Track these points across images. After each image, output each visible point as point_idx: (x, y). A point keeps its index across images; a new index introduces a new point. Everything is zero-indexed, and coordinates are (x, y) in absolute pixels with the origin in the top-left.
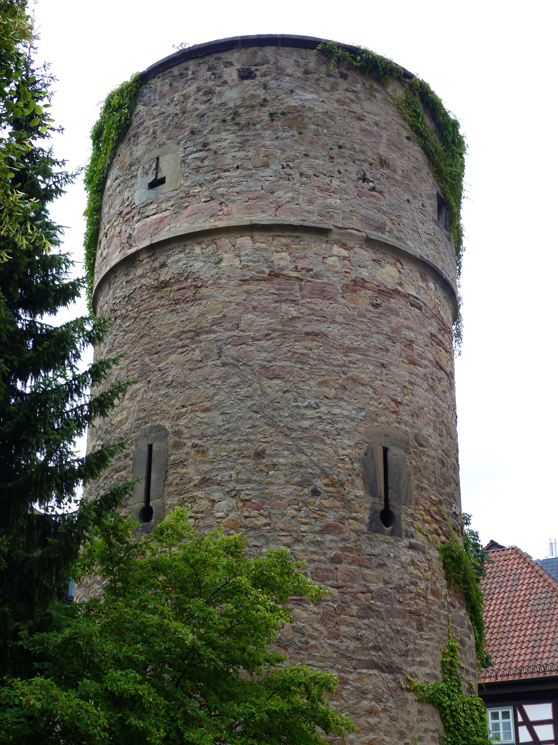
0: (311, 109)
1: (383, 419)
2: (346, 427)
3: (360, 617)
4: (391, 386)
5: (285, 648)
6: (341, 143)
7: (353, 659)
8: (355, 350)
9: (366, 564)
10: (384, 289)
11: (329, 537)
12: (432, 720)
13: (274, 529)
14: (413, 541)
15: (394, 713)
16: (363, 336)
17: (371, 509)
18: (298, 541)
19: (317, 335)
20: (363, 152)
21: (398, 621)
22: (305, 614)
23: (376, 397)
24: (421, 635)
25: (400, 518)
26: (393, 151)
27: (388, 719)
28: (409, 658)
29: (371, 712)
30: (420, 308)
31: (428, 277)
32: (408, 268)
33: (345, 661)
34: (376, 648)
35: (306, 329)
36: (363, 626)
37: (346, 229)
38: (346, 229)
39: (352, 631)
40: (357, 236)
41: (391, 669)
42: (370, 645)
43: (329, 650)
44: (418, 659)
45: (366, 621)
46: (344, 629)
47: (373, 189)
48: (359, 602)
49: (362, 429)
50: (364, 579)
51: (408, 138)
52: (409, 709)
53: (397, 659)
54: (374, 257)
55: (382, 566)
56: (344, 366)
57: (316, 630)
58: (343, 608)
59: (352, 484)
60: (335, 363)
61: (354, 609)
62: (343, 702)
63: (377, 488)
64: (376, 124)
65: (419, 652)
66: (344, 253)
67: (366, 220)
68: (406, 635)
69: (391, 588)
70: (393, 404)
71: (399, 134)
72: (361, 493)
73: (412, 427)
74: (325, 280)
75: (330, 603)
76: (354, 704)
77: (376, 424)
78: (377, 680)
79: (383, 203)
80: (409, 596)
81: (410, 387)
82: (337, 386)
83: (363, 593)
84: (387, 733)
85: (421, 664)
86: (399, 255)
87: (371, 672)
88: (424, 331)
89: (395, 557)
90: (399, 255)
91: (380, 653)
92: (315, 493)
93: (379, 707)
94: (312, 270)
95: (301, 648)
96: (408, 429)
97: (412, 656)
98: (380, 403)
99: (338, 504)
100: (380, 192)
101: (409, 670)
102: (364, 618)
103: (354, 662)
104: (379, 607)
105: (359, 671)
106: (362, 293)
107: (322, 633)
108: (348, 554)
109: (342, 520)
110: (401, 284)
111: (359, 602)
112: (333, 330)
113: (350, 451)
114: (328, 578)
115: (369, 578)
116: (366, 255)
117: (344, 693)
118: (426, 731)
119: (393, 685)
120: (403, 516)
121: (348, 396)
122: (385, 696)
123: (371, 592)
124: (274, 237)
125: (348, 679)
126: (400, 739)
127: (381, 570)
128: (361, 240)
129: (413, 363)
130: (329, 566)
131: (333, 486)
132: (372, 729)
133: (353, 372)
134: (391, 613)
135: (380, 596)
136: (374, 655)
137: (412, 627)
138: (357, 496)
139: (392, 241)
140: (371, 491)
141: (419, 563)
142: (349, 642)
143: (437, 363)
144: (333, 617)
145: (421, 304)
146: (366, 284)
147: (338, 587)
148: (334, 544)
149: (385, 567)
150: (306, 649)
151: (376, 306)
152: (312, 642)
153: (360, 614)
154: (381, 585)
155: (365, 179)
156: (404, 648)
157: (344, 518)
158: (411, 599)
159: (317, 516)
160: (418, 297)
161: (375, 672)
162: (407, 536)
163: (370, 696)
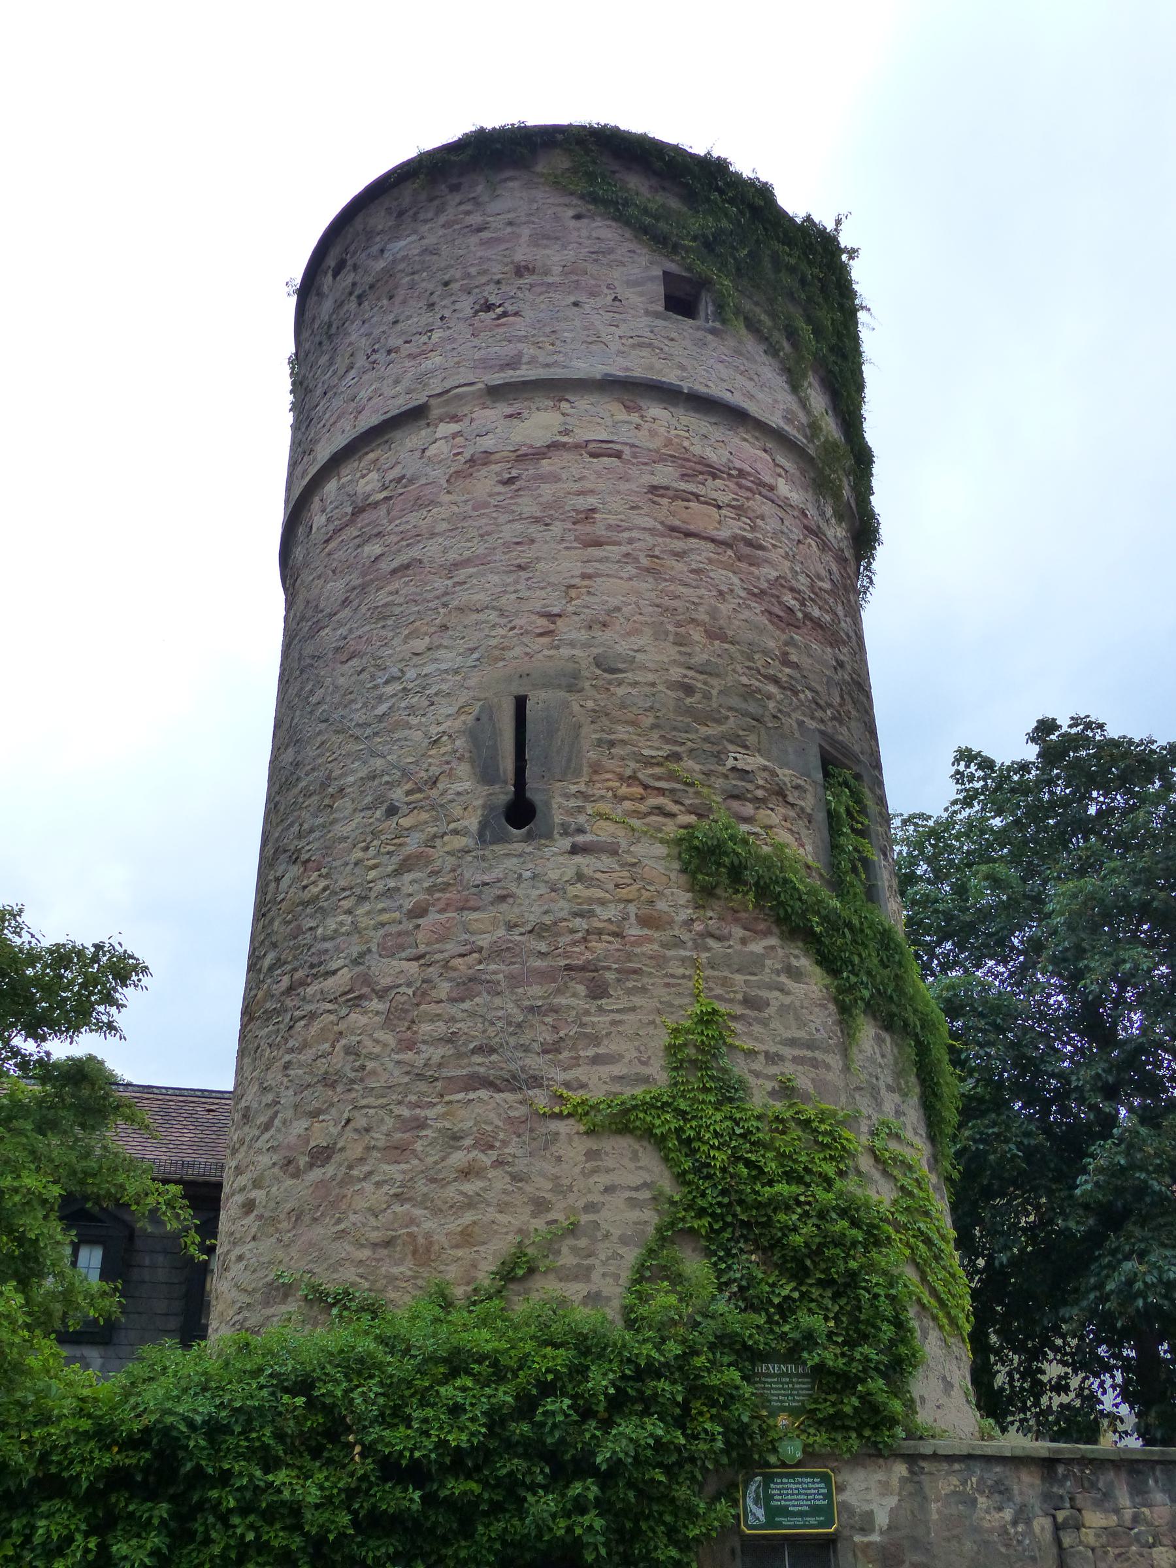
0: (404, 258)
1: (518, 651)
2: (444, 687)
3: (453, 1000)
4: (538, 593)
5: (333, 1086)
6: (447, 277)
7: (437, 1079)
8: (466, 563)
9: (471, 904)
10: (531, 451)
11: (408, 877)
12: (631, 1166)
13: (334, 893)
14: (580, 839)
15: (521, 1166)
16: (481, 536)
17: (484, 806)
18: (363, 899)
19: (407, 567)
20: (485, 272)
21: (536, 990)
22: (364, 1020)
23: (503, 621)
24: (600, 1009)
25: (547, 804)
26: (546, 247)
27: (508, 1179)
28: (565, 1054)
29: (466, 1173)
30: (618, 455)
31: (643, 403)
32: (583, 403)
33: (423, 1086)
34: (485, 1049)
35: (395, 564)
36: (460, 1015)
37: (448, 391)
38: (448, 391)
39: (441, 1028)
40: (473, 393)
41: (511, 1083)
42: (471, 1046)
43: (396, 1073)
44: (591, 1052)
45: (466, 1005)
46: (425, 1028)
47: (505, 314)
48: (454, 974)
49: (471, 682)
50: (467, 931)
51: (578, 217)
52: (561, 1152)
53: (535, 1062)
54: (509, 410)
55: (503, 898)
56: (446, 594)
57: (377, 1041)
58: (422, 995)
59: (450, 776)
60: (430, 596)
61: (444, 988)
62: (416, 1162)
63: (498, 770)
64: (510, 224)
65: (595, 1040)
66: (454, 427)
67: (485, 364)
68: (556, 1012)
69: (522, 934)
70: (543, 622)
71: (556, 218)
72: (467, 785)
73: (586, 646)
74: (423, 481)
75: (403, 989)
76: (436, 1163)
77: (501, 664)
78: (487, 1109)
79: (520, 326)
80: (567, 939)
81: (586, 582)
82: (433, 629)
83: (462, 955)
84: (502, 1208)
85: (596, 1060)
86: (557, 388)
87: (472, 1095)
88: (623, 486)
89: (534, 877)
90: (557, 388)
91: (494, 1057)
92: (392, 811)
93: (486, 1159)
94: (403, 477)
95: (353, 1081)
96: (577, 652)
97: (574, 1048)
98: (512, 629)
99: (425, 816)
100: (516, 314)
101: (561, 1076)
102: (463, 1000)
103: (439, 1084)
104: (495, 973)
105: (447, 1098)
106: (484, 472)
107: (385, 1045)
108: (437, 895)
109: (430, 842)
110: (566, 432)
111: (454, 974)
112: (432, 549)
113: (449, 723)
114: (402, 948)
115: (475, 926)
116: (491, 415)
117: (419, 1146)
118: (609, 1190)
119: (521, 1111)
120: (557, 801)
121: (451, 637)
122: (502, 1136)
123: (480, 950)
124: (360, 459)
125: (426, 1118)
126: (534, 1215)
127: (504, 907)
128: (480, 397)
129: (598, 544)
130: (408, 925)
131: (420, 790)
132: (471, 1203)
133: (462, 597)
134: (514, 981)
135: (498, 952)
136: (480, 1065)
137: (574, 995)
138: (459, 794)
139: (544, 373)
140: (487, 774)
141: (598, 875)
142: (431, 1050)
143: (673, 529)
144: (406, 1011)
145: (618, 447)
146: (493, 458)
147: (417, 958)
148: (416, 886)
149: (511, 900)
150: (362, 1080)
151: (510, 481)
152: (370, 1065)
153: (454, 995)
154: (501, 932)
155: (488, 307)
156: (550, 1038)
157: (435, 836)
158: (574, 943)
159: (391, 848)
160: (615, 438)
161: (483, 1094)
162: (565, 833)
163: (468, 1142)
